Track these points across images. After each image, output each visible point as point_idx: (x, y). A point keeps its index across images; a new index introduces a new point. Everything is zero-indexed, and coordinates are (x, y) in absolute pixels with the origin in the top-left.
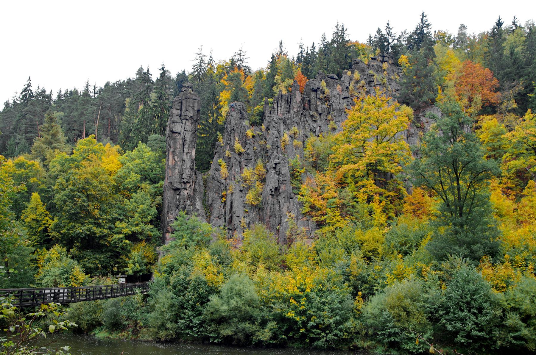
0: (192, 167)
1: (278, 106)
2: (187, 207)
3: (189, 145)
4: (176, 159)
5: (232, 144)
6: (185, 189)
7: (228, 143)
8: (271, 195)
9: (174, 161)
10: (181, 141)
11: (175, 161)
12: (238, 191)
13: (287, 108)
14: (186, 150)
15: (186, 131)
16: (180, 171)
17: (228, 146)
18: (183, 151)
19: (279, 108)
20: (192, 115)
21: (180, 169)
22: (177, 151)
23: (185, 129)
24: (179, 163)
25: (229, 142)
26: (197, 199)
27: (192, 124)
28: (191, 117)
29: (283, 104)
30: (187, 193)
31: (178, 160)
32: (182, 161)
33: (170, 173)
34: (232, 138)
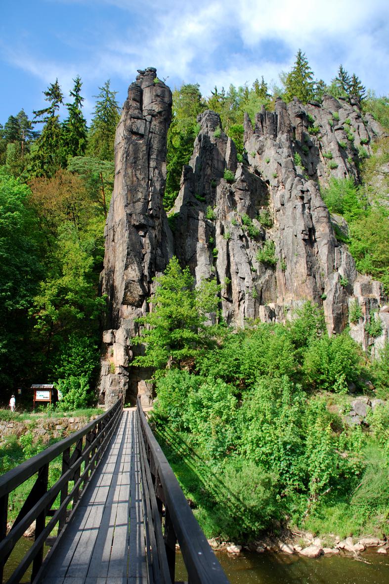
0: (162, 192)
1: (262, 126)
2: (158, 258)
3: (157, 156)
4: (139, 176)
5: (216, 166)
6: (154, 228)
7: (208, 164)
8: (304, 240)
9: (135, 179)
10: (144, 148)
11: (138, 178)
12: (236, 237)
13: (274, 129)
14: (153, 164)
15: (152, 132)
16: (146, 196)
17: (209, 169)
18: (149, 164)
19: (264, 128)
20: (160, 110)
21: (144, 192)
22: (140, 162)
23: (151, 130)
24: (142, 182)
25: (210, 162)
26: (168, 249)
27: (160, 123)
28: (160, 113)
29: (268, 123)
30: (156, 236)
31: (142, 177)
32: (147, 181)
33: (129, 198)
34: (215, 157)
